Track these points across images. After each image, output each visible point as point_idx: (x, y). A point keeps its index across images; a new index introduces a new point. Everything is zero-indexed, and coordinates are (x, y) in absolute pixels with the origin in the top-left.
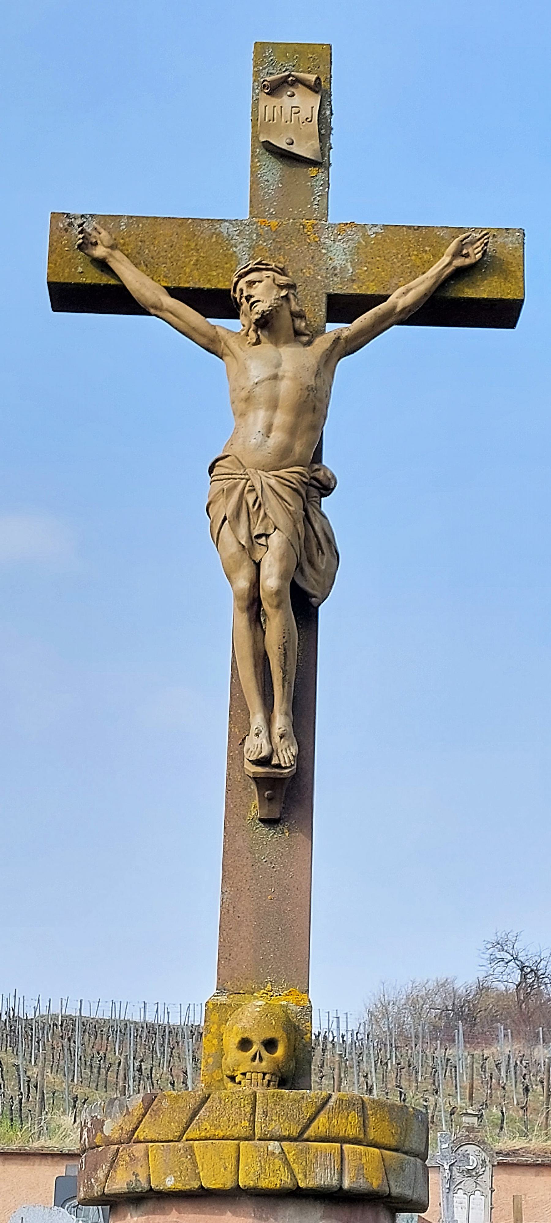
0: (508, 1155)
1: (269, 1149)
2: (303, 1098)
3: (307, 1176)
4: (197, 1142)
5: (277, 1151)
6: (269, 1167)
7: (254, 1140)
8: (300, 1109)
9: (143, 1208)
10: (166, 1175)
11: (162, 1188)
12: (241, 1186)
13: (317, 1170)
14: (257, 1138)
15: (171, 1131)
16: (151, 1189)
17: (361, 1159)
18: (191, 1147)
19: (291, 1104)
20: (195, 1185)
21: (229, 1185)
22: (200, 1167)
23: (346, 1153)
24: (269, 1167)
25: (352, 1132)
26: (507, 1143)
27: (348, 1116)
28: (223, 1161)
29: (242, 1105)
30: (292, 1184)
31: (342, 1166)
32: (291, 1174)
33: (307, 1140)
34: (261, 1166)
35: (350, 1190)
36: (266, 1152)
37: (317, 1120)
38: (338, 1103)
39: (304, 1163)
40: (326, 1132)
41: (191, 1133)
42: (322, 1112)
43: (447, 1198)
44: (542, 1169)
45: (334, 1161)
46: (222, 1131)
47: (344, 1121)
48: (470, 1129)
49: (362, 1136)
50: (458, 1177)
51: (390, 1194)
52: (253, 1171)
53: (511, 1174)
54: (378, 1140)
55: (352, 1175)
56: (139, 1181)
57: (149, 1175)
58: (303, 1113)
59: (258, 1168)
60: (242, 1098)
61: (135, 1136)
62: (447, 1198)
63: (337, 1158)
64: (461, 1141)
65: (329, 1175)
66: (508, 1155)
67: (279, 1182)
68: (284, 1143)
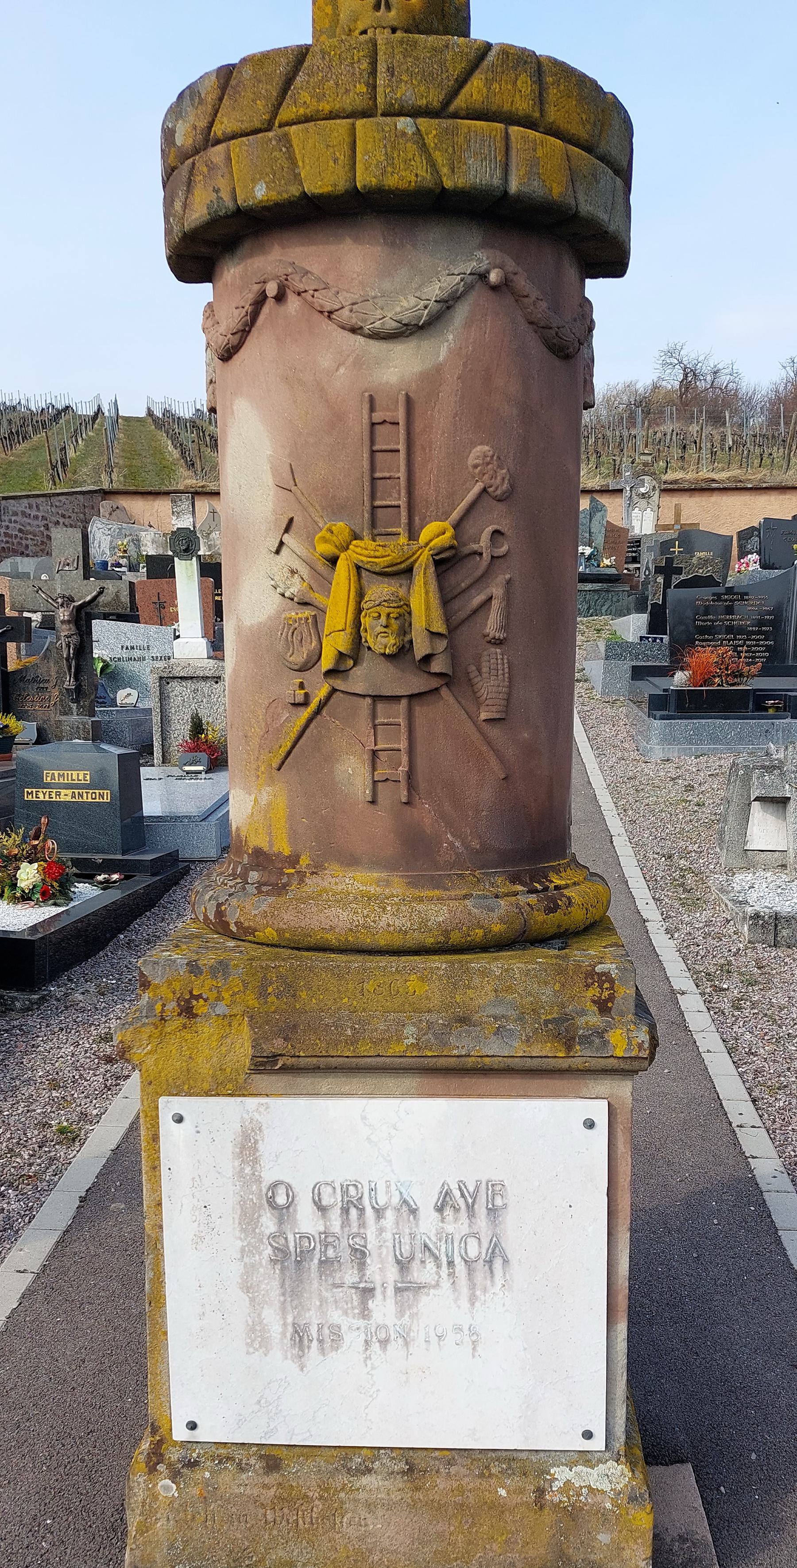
0: (671, 483)
1: (398, 127)
2: (447, 47)
3: (456, 170)
4: (294, 127)
5: (410, 131)
6: (399, 156)
7: (376, 116)
8: (442, 63)
9: (240, 252)
10: (254, 181)
11: (251, 203)
12: (359, 187)
13: (470, 162)
14: (380, 112)
15: (257, 114)
16: (238, 208)
17: (535, 150)
18: (286, 135)
19: (428, 55)
20: (294, 191)
21: (342, 186)
22: (300, 163)
23: (513, 138)
24: (399, 156)
25: (523, 105)
26: (670, 476)
27: (517, 79)
28: (332, 150)
29: (356, 58)
30: (433, 182)
31: (507, 159)
32: (431, 166)
33: (455, 116)
34: (386, 153)
35: (519, 196)
36: (393, 131)
37: (469, 83)
38: (501, 57)
39: (450, 150)
40: (483, 103)
41: (285, 114)
42: (477, 72)
43: (628, 511)
44: (693, 492)
45: (496, 149)
46: (328, 102)
47: (509, 87)
48: (645, 464)
49: (537, 115)
50: (635, 499)
51: (577, 212)
52: (375, 162)
53: (672, 497)
54: (562, 126)
55: (521, 174)
56: (221, 198)
57: (234, 189)
58: (447, 71)
59: (383, 158)
60: (355, 48)
61: (212, 134)
62: (628, 511)
63: (500, 144)
64: (639, 473)
65: (488, 169)
66: (671, 483)
67: (413, 178)
68: (420, 121)
